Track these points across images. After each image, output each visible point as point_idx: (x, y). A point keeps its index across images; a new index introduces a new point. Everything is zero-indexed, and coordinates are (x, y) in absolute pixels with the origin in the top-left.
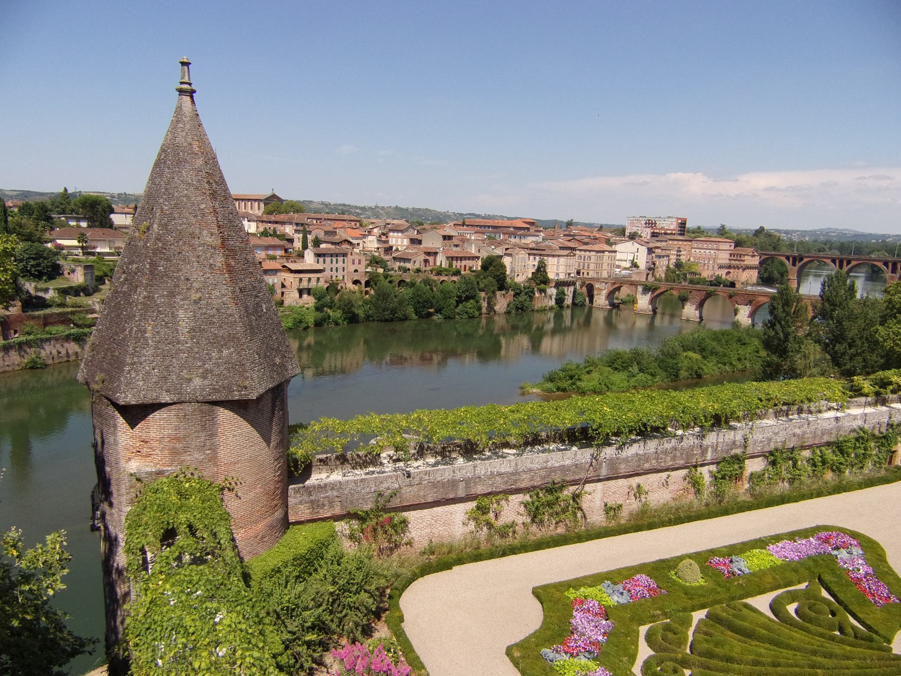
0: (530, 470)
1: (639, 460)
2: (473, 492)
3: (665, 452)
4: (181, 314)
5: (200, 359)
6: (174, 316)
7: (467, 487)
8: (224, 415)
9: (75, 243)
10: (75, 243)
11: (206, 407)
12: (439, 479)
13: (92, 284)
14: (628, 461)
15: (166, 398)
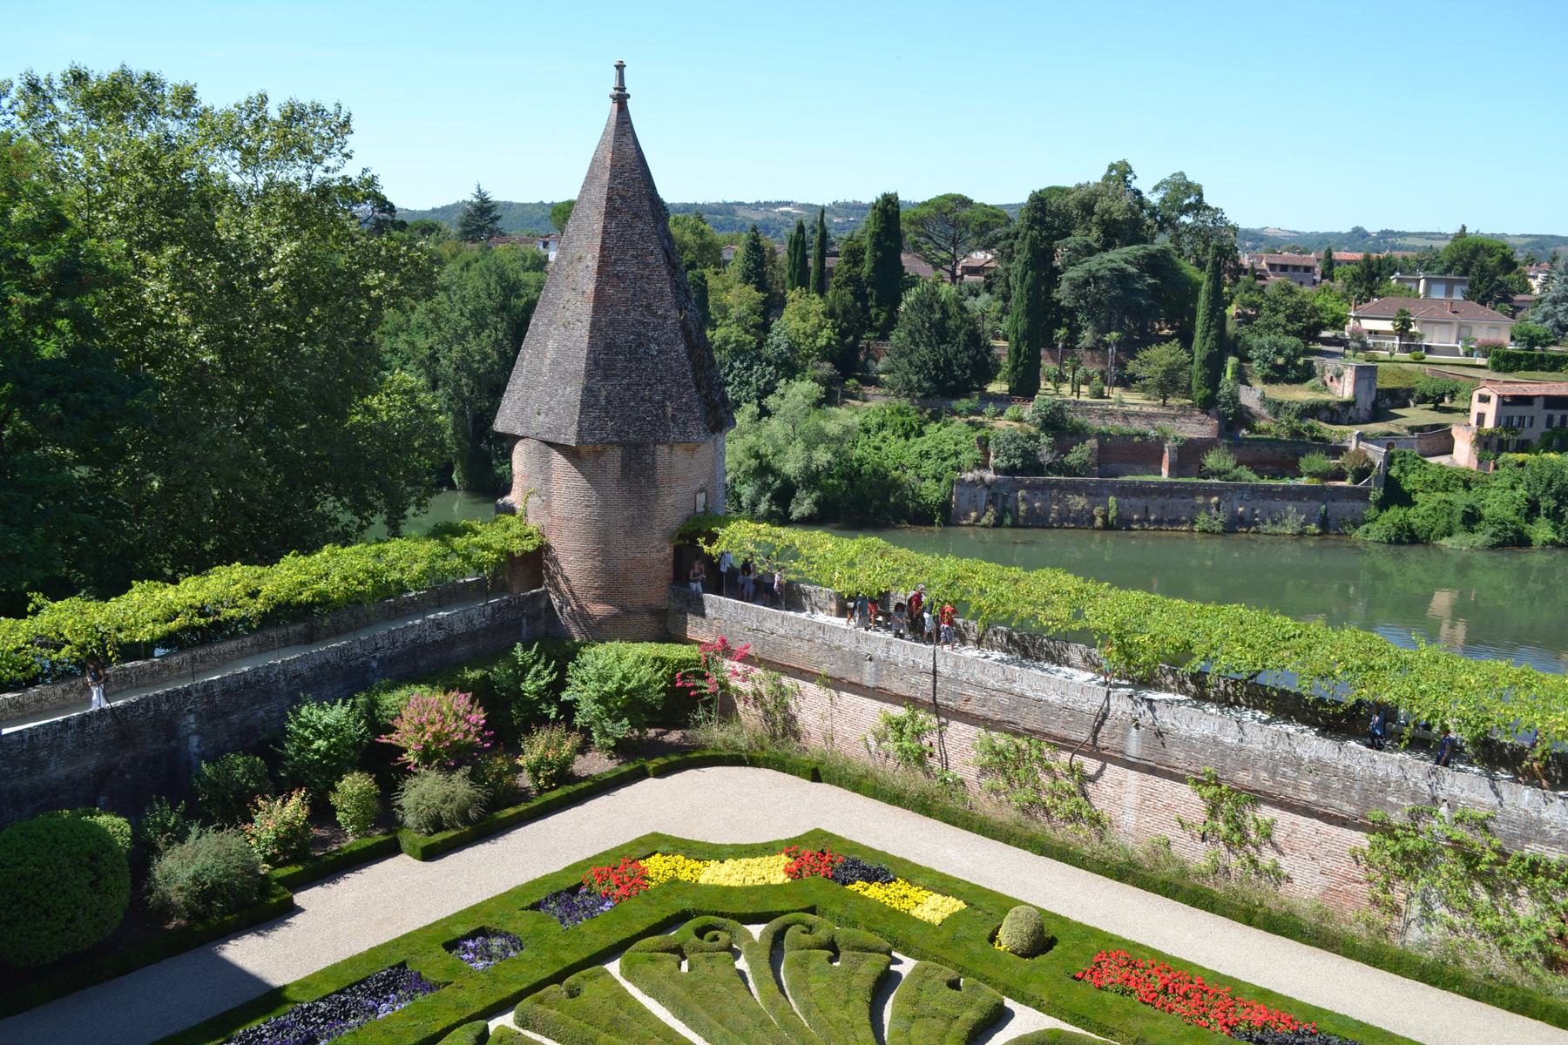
0: (980, 686)
1: (1223, 756)
2: (884, 684)
3: (1297, 763)
4: (551, 344)
5: (549, 394)
6: (546, 346)
7: (878, 673)
8: (558, 459)
9: (1387, 326)
10: (1387, 326)
11: (544, 447)
12: (837, 643)
13: (1365, 403)
14: (1192, 747)
15: (519, 431)
